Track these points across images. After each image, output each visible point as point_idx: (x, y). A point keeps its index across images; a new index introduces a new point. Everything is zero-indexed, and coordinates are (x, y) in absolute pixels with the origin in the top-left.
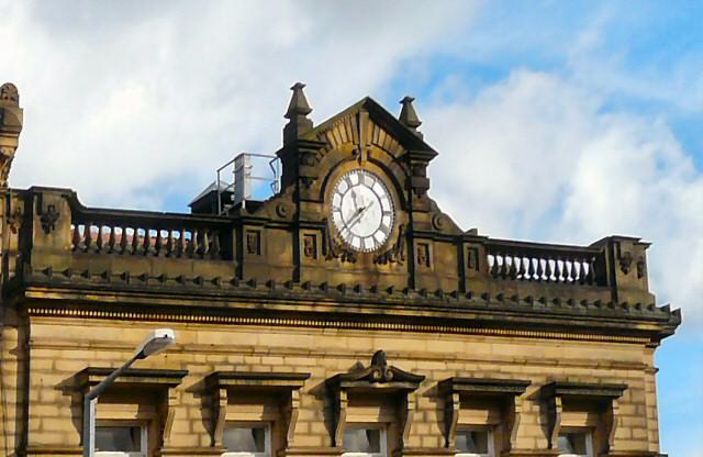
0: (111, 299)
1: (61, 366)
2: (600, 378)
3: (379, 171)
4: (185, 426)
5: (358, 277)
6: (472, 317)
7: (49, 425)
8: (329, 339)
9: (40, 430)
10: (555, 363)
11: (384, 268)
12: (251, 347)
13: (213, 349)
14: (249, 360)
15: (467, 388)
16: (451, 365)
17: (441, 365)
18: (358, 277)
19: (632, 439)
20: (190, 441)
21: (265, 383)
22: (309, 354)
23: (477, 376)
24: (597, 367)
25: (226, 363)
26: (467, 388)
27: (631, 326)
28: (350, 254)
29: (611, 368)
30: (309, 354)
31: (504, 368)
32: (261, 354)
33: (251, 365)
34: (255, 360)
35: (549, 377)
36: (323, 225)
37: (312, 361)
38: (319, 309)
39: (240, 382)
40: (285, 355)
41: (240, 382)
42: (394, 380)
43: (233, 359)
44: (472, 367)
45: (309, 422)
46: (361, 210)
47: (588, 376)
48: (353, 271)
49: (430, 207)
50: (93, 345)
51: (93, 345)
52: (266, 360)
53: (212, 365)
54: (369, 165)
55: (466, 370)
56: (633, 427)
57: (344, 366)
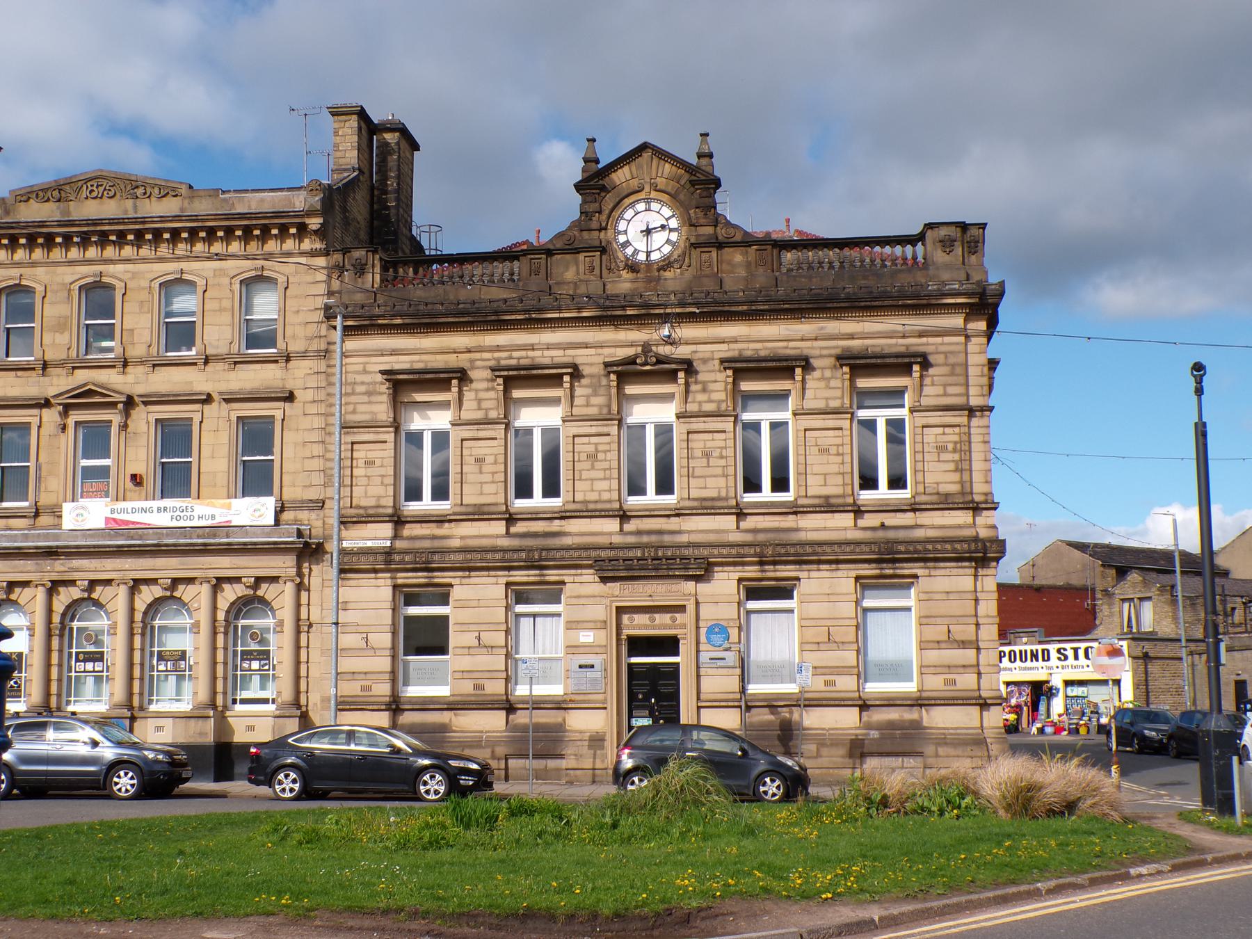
0: (399, 321)
1: (370, 368)
2: (907, 346)
3: (665, 197)
4: (474, 405)
5: (636, 285)
6: (745, 308)
7: (361, 408)
8: (606, 334)
9: (354, 412)
10: (851, 337)
11: (668, 274)
12: (533, 345)
13: (498, 349)
14: (531, 354)
15: (738, 365)
16: (733, 346)
17: (724, 347)
18: (636, 285)
19: (945, 394)
20: (479, 415)
21: (535, 372)
22: (586, 346)
23: (763, 353)
24: (904, 337)
25: (511, 358)
26: (738, 365)
27: (934, 302)
28: (633, 267)
29: (920, 336)
30: (586, 346)
31: (792, 344)
32: (542, 349)
33: (533, 358)
34: (538, 353)
35: (845, 349)
36: (603, 250)
37: (593, 351)
38: (585, 314)
39: (511, 373)
40: (564, 349)
41: (511, 373)
42: (659, 362)
43: (515, 354)
44: (753, 346)
45: (588, 397)
46: (648, 230)
47: (890, 346)
48: (632, 281)
49: (717, 220)
50: (394, 352)
51: (394, 352)
52: (546, 353)
53: (498, 360)
54: (654, 194)
55: (749, 349)
56: (945, 386)
57: (630, 352)
